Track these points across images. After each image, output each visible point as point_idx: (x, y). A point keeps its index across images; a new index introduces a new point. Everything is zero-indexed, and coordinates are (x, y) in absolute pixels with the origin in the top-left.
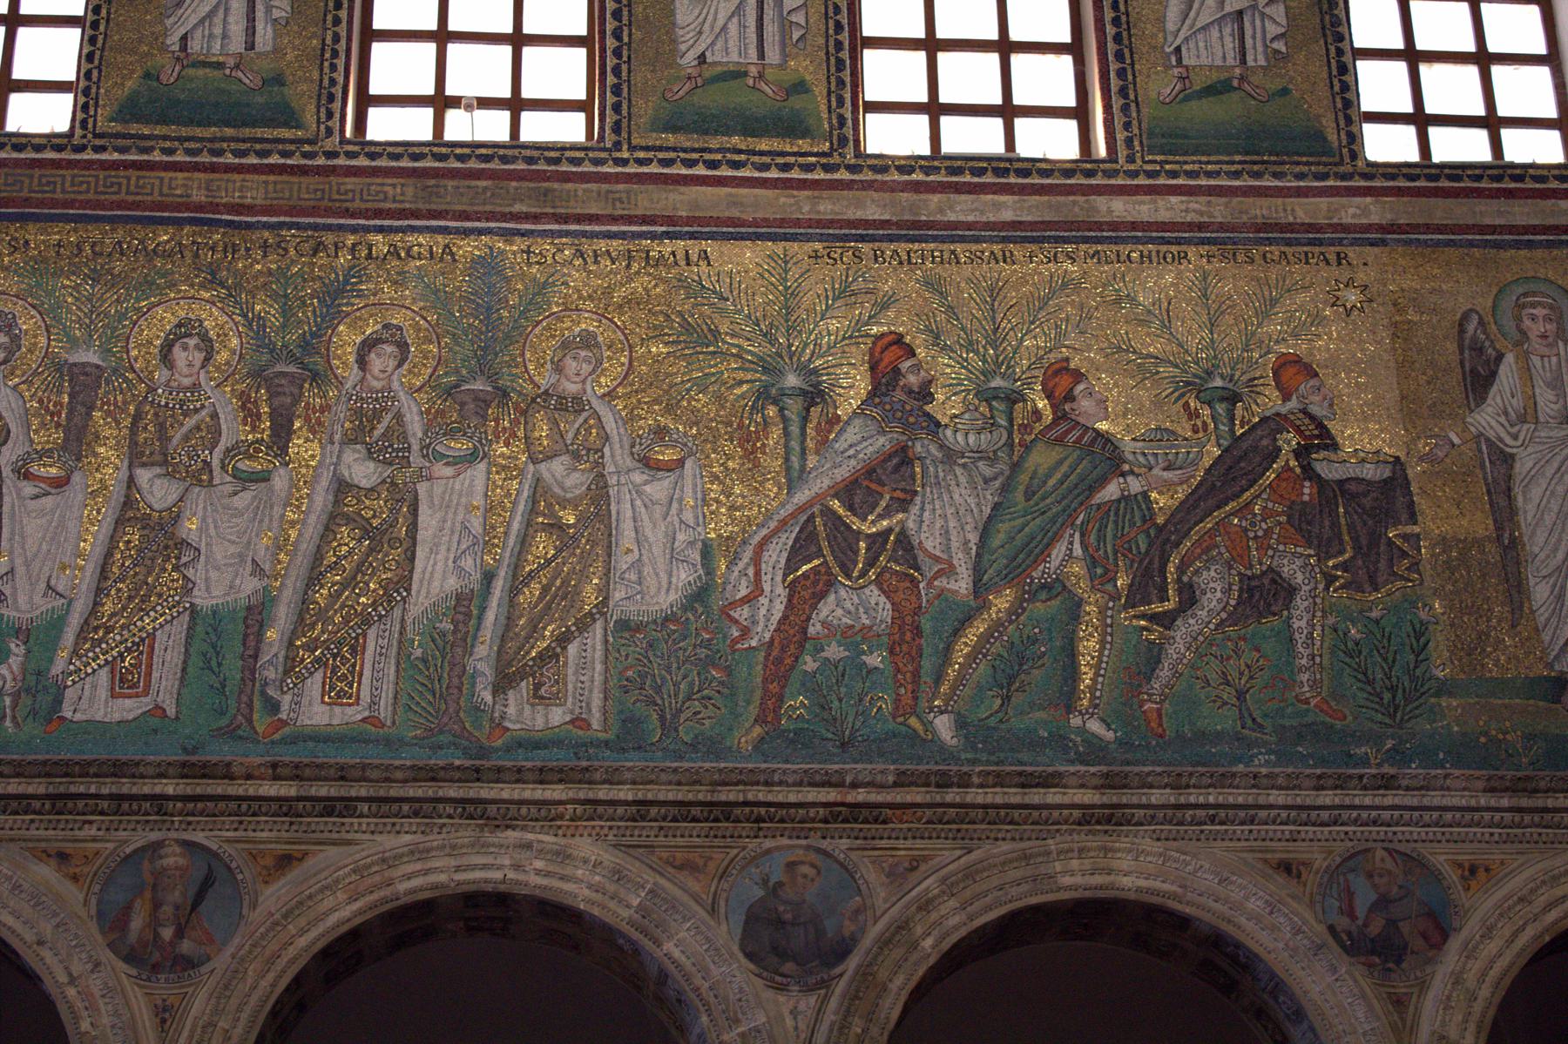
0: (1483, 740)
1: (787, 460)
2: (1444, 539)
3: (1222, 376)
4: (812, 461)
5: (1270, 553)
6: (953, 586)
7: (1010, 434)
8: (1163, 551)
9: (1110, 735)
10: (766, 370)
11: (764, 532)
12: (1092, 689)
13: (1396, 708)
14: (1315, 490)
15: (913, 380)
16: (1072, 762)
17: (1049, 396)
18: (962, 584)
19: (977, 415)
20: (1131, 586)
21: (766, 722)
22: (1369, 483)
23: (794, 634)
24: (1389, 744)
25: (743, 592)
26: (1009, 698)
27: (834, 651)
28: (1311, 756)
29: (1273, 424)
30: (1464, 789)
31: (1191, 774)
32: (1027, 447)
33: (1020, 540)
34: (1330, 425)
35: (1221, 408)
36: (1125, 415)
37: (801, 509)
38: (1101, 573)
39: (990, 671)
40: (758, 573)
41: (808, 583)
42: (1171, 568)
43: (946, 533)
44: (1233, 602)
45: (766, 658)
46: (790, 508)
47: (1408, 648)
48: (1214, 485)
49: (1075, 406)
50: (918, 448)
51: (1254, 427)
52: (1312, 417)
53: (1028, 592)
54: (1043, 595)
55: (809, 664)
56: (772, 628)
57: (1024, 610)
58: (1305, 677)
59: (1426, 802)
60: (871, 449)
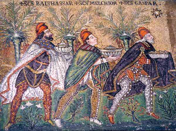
4: (22, 55)
5: (139, 77)
6: (59, 87)
8: (112, 77)
9: (100, 124)
10: (9, 32)
11: (10, 74)
13: (171, 115)
14: (150, 61)
15: (48, 35)
18: (61, 86)
19: (64, 43)
21: (11, 122)
22: (163, 59)
23: (18, 100)
24: (170, 124)
25: (5, 89)
27: (29, 104)
33: (76, 75)
34: (154, 46)
35: (126, 41)
39: (69, 107)
40: (9, 85)
41: (22, 87)
44: (130, 89)
45: (11, 107)
46: (16, 68)
47: (174, 100)
48: (125, 60)
49: (89, 41)
51: (134, 46)
52: (148, 43)
53: (79, 88)
54: (83, 88)
55: (22, 108)
56: (13, 98)
58: (148, 108)
60: (37, 52)
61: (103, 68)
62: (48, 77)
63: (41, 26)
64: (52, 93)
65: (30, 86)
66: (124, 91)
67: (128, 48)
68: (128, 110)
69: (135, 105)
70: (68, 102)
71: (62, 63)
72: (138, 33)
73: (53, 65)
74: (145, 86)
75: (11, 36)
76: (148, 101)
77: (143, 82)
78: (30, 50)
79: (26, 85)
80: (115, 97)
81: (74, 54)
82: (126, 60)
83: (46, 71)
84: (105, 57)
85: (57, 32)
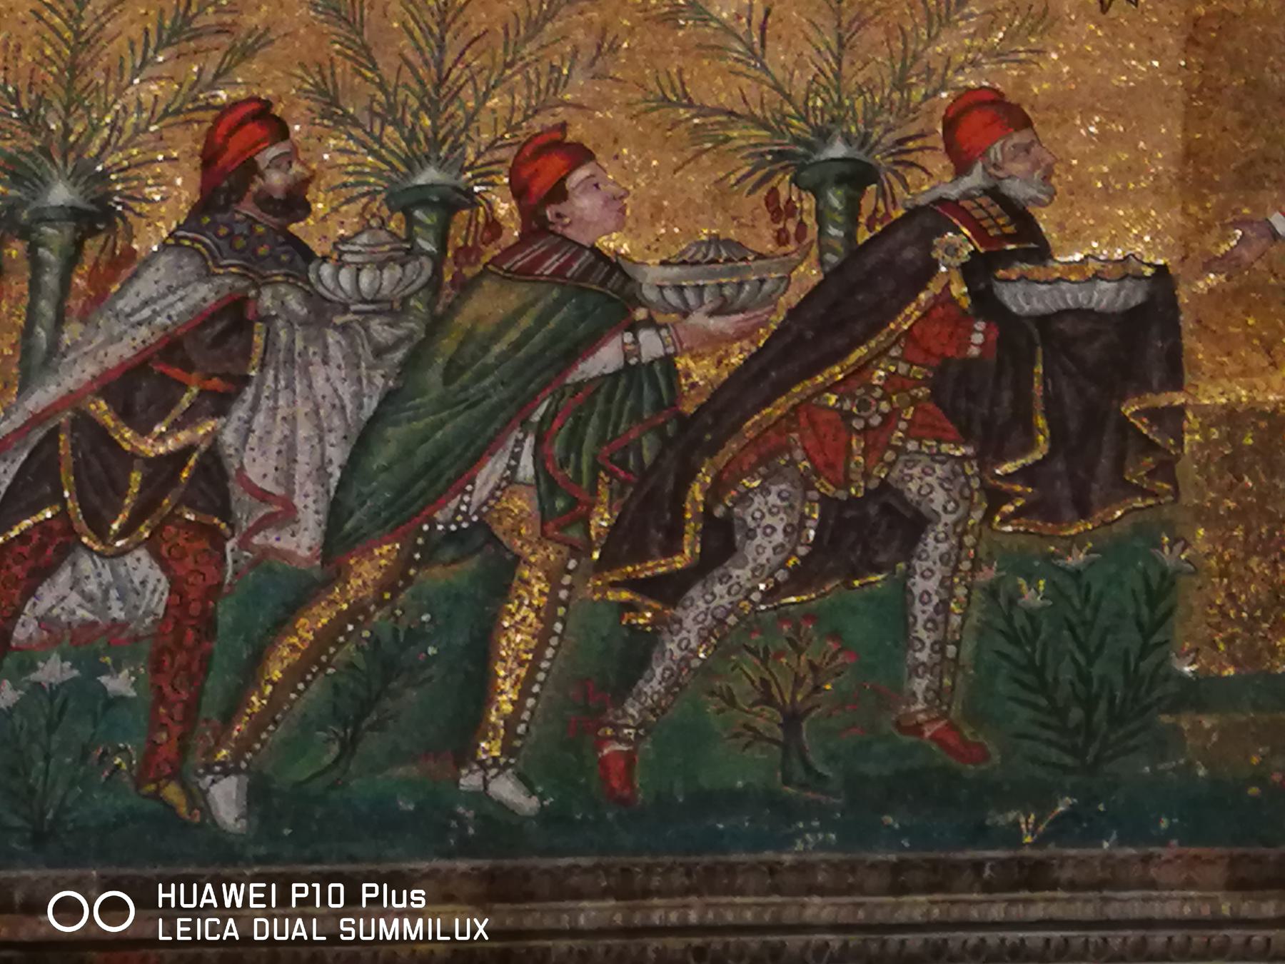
0: (1254, 791)
1: (28, 332)
2: (1231, 417)
3: (848, 140)
5: (889, 456)
6: (285, 542)
7: (437, 272)
12: (510, 722)
14: (994, 335)
15: (276, 180)
16: (449, 855)
17: (519, 191)
18: (302, 541)
19: (383, 235)
20: (613, 528)
26: (354, 740)
27: (54, 670)
28: (904, 831)
29: (934, 217)
30: (1189, 884)
31: (649, 870)
32: (465, 287)
33: (423, 453)
34: (1045, 219)
35: (835, 199)
36: (654, 218)
37: (36, 420)
38: (561, 505)
42: (696, 493)
43: (289, 452)
44: (802, 551)
46: (18, 419)
49: (563, 208)
50: (267, 300)
54: (449, 553)
57: (409, 580)
59: (1113, 911)
60: (180, 306)
61: (629, 403)
62: (224, 476)
63: (241, 124)
64: (226, 589)
65: (85, 545)
66: (751, 565)
67: (838, 246)
68: (755, 704)
69: (817, 661)
70: (332, 650)
71: (334, 373)
72: (937, 140)
73: (277, 391)
74: (929, 521)
75: (26, 204)
76: (923, 634)
77: (909, 496)
78: (132, 292)
79: (60, 539)
80: (679, 612)
81: (440, 309)
82: (809, 334)
83: (214, 437)
84: (660, 319)
85: (343, 160)
